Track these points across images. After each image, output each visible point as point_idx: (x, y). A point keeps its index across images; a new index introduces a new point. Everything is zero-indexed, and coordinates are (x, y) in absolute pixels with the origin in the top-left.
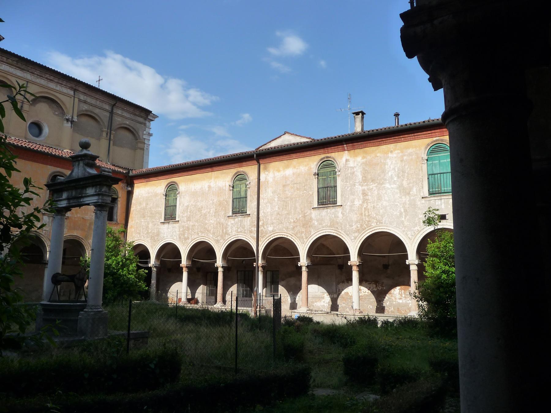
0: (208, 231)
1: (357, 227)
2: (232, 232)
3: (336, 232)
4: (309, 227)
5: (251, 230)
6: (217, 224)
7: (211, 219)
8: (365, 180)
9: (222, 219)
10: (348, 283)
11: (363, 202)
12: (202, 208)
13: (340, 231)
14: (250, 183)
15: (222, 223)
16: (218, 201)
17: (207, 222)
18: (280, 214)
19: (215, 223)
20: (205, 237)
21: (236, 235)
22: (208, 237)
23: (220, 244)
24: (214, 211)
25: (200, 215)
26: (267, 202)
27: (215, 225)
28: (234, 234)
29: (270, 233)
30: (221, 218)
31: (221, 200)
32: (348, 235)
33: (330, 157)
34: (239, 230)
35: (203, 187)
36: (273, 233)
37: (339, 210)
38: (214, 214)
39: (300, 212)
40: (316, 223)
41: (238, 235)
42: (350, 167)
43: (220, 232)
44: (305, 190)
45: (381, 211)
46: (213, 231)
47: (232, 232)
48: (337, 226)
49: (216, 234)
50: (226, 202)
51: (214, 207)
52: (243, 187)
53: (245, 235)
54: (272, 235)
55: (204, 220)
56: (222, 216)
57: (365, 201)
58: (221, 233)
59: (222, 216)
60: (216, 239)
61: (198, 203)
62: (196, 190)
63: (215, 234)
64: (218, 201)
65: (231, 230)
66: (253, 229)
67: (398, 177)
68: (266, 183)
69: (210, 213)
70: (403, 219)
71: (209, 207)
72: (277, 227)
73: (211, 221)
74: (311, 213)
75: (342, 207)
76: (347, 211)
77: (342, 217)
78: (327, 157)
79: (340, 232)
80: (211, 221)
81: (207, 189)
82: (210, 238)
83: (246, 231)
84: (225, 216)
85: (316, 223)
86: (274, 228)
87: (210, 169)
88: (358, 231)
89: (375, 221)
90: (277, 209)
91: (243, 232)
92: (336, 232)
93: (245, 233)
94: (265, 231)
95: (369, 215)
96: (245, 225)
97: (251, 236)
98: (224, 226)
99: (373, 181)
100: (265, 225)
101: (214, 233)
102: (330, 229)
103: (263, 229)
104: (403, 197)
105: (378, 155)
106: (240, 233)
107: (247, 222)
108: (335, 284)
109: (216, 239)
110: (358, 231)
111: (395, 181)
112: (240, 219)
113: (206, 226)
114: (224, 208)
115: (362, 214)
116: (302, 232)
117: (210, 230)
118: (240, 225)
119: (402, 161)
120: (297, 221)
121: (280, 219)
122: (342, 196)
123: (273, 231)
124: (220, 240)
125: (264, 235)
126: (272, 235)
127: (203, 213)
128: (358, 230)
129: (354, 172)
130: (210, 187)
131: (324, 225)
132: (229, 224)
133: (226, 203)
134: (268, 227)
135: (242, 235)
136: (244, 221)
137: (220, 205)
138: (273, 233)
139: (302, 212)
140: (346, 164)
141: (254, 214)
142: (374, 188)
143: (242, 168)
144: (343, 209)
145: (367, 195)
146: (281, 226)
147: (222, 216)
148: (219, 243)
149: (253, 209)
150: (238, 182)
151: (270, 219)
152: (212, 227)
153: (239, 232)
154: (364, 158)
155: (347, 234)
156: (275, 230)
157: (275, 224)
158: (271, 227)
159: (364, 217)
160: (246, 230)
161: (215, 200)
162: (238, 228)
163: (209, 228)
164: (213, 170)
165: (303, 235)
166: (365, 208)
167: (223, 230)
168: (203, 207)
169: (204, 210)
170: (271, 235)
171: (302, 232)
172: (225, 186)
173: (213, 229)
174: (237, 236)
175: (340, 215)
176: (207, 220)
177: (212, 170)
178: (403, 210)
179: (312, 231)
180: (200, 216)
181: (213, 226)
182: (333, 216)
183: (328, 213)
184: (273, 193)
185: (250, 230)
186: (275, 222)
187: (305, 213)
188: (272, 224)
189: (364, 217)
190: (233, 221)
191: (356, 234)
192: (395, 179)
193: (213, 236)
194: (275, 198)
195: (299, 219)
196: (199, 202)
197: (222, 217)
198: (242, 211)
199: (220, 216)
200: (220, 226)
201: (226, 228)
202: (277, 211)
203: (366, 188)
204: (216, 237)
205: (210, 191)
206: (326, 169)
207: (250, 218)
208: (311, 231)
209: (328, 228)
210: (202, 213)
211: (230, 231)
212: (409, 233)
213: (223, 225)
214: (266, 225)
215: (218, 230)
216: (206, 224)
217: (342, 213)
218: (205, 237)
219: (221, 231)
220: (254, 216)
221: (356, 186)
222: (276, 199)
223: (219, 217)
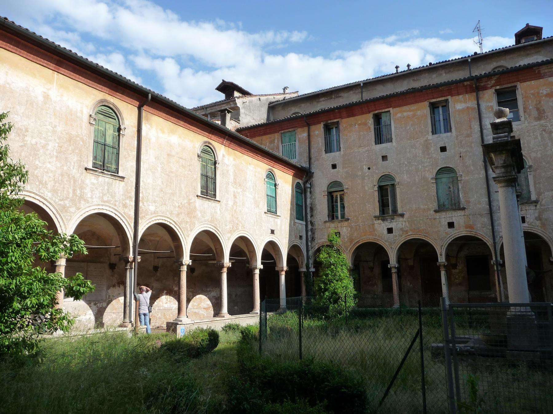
0: (41, 182)
1: (230, 227)
2: (92, 198)
3: (215, 229)
4: (194, 217)
5: (126, 203)
6: (62, 175)
7: (50, 162)
8: (235, 183)
9: (73, 168)
10: (120, 287)
11: (234, 204)
12: (27, 130)
13: (219, 229)
14: (125, 128)
15: (74, 177)
16: (67, 134)
17: (40, 165)
18: (163, 191)
19: (59, 172)
20: (34, 193)
21: (99, 205)
22: (42, 195)
23: (69, 214)
24: (57, 148)
25: (20, 144)
26: (148, 168)
27: (57, 175)
28: (96, 203)
29: (151, 214)
30: (72, 168)
31: (71, 134)
32: (224, 234)
33: (211, 144)
34: (105, 198)
35: (31, 89)
36: (154, 215)
37: (217, 205)
38: (55, 153)
39: (185, 196)
40: (200, 215)
41: (102, 205)
42: (227, 164)
43: (68, 191)
44: (190, 170)
45: (244, 217)
46: (54, 186)
47: (92, 198)
48: (216, 223)
49: (59, 194)
50: (83, 142)
51: (55, 140)
52: (109, 128)
53: (116, 208)
54: (153, 217)
55: (31, 158)
56: (72, 164)
57: (235, 203)
58: (71, 195)
59: (72, 164)
60: (62, 203)
61: (16, 116)
62: (12, 86)
63: (58, 193)
64: (67, 134)
65: (90, 193)
66: (128, 201)
67: (253, 190)
68: (148, 140)
69: (47, 150)
70: (256, 228)
71: (44, 136)
72: (160, 208)
73: (49, 166)
74: (195, 202)
75: (220, 203)
76: (224, 209)
77: (220, 214)
78: (209, 143)
79: (218, 230)
80: (49, 166)
81: (41, 99)
82: (47, 198)
83: (117, 203)
84: (80, 166)
85: (200, 215)
86: (156, 209)
87: (52, 66)
88: (230, 232)
89: (241, 225)
90: (160, 184)
91: (112, 202)
92: (215, 229)
93: (115, 205)
94: (145, 211)
95: (237, 218)
96: (115, 194)
97: (124, 213)
98: (77, 184)
99: (240, 185)
100: (145, 201)
101: (54, 191)
102: (211, 225)
103: (143, 206)
104: (256, 208)
105: (243, 162)
106: (107, 204)
107: (119, 189)
108: (105, 289)
109: (62, 203)
110: (230, 232)
111: (251, 192)
112: (107, 179)
113: (36, 171)
114: (77, 151)
115: (233, 215)
116: (187, 222)
117: (46, 182)
118: (108, 190)
119: (255, 176)
120: (182, 206)
121: (163, 198)
122: (220, 191)
123: (155, 213)
124: (70, 207)
125: (143, 215)
126: (153, 217)
127: (29, 142)
128: (231, 231)
129: (228, 170)
130: (47, 97)
131: (206, 218)
132: (88, 182)
133: (81, 143)
134: (149, 205)
135: (110, 207)
136: (114, 186)
137: (70, 141)
138: (154, 215)
139: (187, 197)
140: (223, 159)
141: (130, 179)
142: (241, 193)
143: (113, 98)
144: (221, 205)
145: (236, 198)
146: (164, 208)
147: (74, 163)
148: (66, 211)
149: (129, 172)
150: (102, 116)
151: (151, 194)
152: (50, 177)
153: (104, 202)
154: (234, 160)
155: (223, 233)
156: (157, 211)
157: (158, 203)
158: (152, 205)
159: (234, 219)
160: (117, 201)
161: (59, 129)
162: (104, 195)
163: (43, 177)
164: (59, 69)
165: (188, 226)
166: (235, 210)
167: (74, 191)
168: (30, 130)
169: (32, 137)
170: (151, 218)
171: (187, 222)
172: (82, 112)
173: (52, 183)
174: (101, 207)
175: (219, 212)
176: (39, 161)
177: (55, 67)
178: (255, 220)
179: (196, 222)
180: (21, 146)
181: (52, 177)
182: (213, 210)
183: (206, 205)
184: (156, 159)
185: (124, 202)
186: (157, 200)
187: (189, 200)
188: (155, 202)
189: (234, 219)
190: (95, 179)
191: (229, 235)
192: (252, 190)
193: (53, 195)
194: (158, 167)
195: (184, 205)
196: (17, 115)
197: (74, 166)
198: (107, 167)
199: (70, 163)
200: (70, 182)
201: (81, 188)
202: (160, 186)
203: (235, 189)
204: (61, 200)
205: (47, 105)
206: (206, 154)
207: (123, 183)
208: (194, 223)
209: (209, 223)
210: (27, 141)
211: (89, 195)
212: (258, 241)
213: (75, 181)
214: (147, 201)
215: (64, 188)
216: (37, 168)
217: (220, 210)
218: (34, 193)
219: (71, 191)
220: (129, 182)
221: (230, 186)
222: (159, 169)
223: (66, 163)
